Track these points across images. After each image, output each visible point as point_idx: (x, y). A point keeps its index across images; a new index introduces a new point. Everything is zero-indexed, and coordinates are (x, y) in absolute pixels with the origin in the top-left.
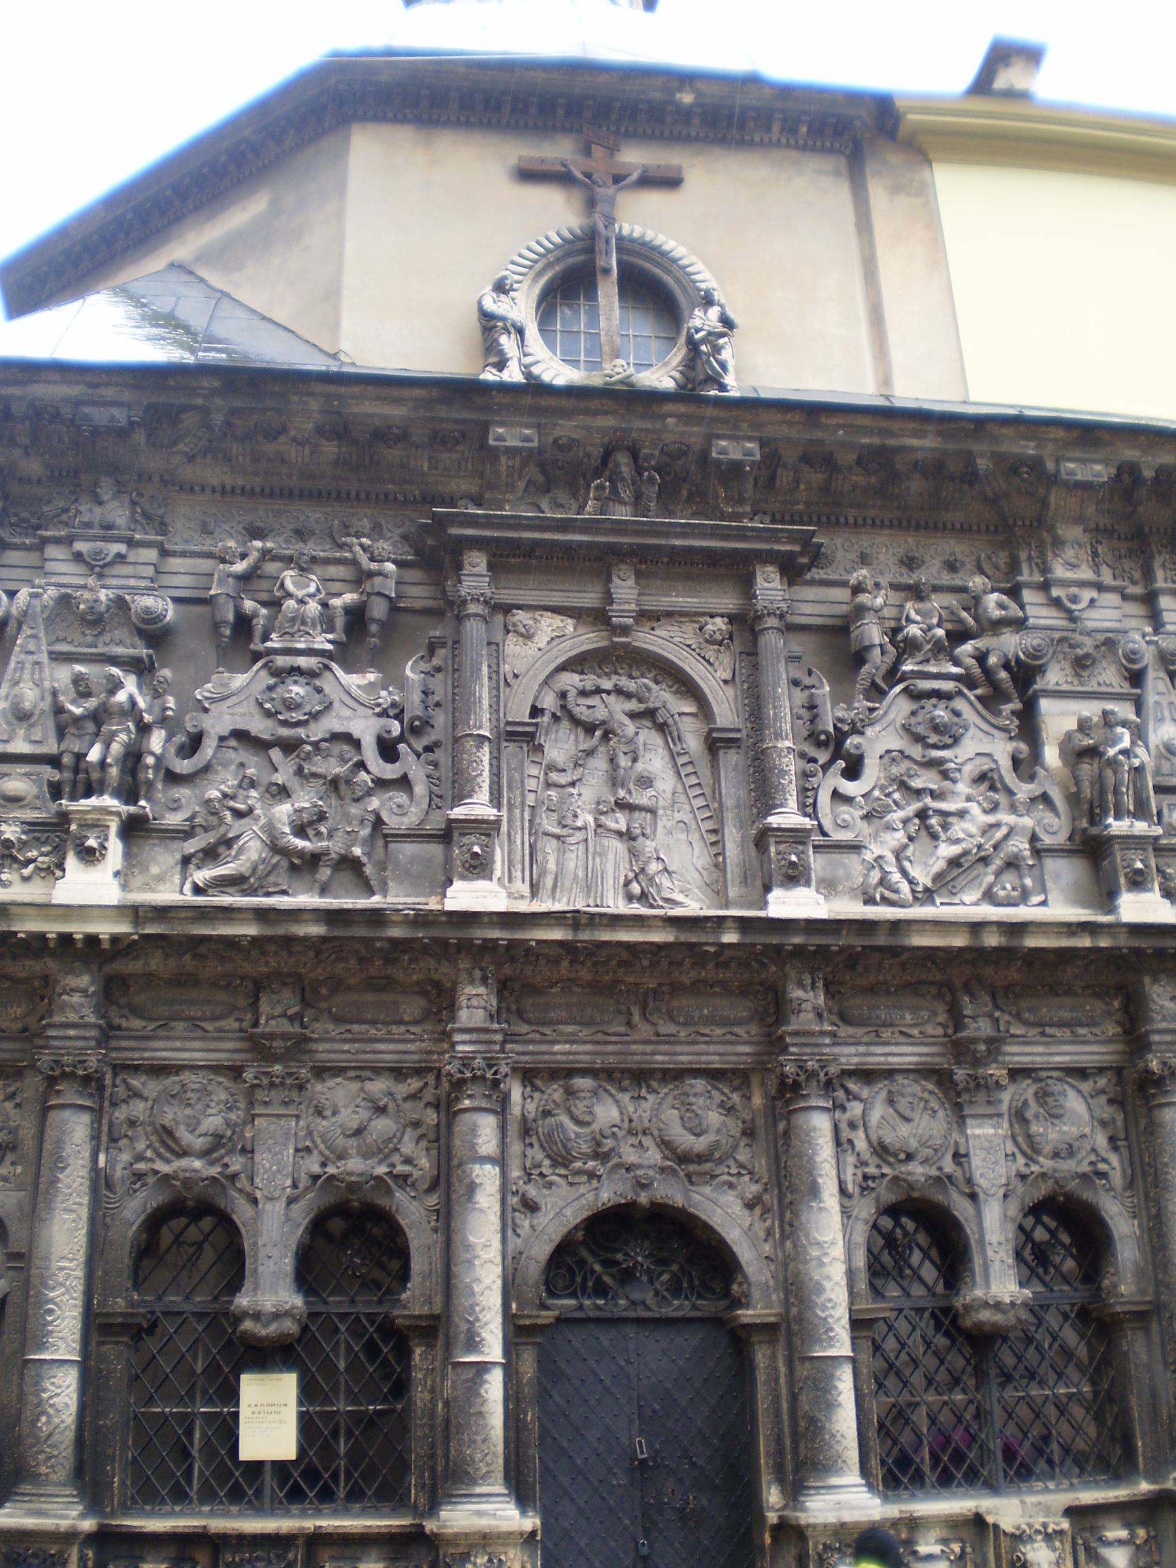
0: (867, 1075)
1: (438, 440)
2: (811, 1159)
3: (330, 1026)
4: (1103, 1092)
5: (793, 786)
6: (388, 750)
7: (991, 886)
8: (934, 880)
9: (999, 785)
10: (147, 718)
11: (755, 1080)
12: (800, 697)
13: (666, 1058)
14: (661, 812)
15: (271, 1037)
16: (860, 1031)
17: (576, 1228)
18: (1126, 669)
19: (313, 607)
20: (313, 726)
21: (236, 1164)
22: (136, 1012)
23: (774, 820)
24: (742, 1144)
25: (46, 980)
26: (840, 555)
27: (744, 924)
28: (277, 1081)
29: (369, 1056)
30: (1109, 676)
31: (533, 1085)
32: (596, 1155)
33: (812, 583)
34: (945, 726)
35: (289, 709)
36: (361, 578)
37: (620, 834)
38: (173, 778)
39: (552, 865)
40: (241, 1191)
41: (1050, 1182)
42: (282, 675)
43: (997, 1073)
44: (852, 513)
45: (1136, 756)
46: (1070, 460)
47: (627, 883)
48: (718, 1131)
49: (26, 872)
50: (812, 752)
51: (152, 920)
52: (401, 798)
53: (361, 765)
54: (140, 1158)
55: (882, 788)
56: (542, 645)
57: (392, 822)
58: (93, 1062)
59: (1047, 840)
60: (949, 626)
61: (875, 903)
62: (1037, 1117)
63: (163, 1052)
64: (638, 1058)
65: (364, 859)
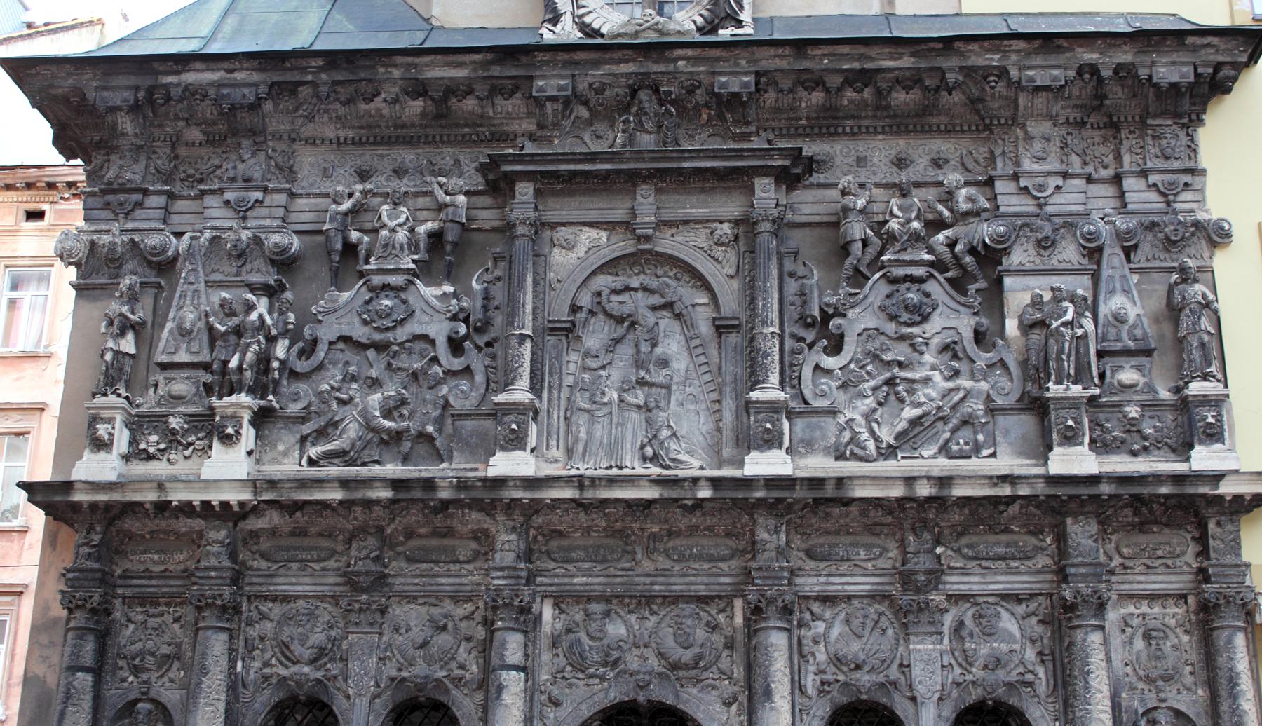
0: (828, 599)
1: (497, 89)
2: (767, 667)
3: (404, 565)
4: (1033, 614)
5: (777, 365)
6: (456, 346)
7: (947, 441)
8: (896, 438)
9: (961, 355)
10: (274, 332)
11: (738, 604)
12: (792, 286)
13: (662, 588)
14: (674, 387)
15: (358, 574)
16: (822, 565)
17: (590, 718)
18: (1084, 248)
19: (402, 235)
20: (399, 331)
21: (335, 669)
22: (264, 556)
23: (754, 395)
24: (724, 655)
25: (200, 534)
26: (839, 160)
27: (715, 482)
28: (364, 607)
29: (434, 588)
30: (1069, 253)
31: (560, 608)
32: (605, 664)
33: (811, 186)
34: (915, 306)
35: (380, 317)
36: (442, 207)
37: (639, 407)
38: (294, 375)
39: (583, 435)
40: (338, 689)
41: (980, 690)
43: (937, 598)
44: (849, 122)
46: (1030, 68)
47: (643, 447)
48: (702, 646)
49: (187, 453)
50: (802, 333)
51: (267, 490)
52: (464, 385)
53: (435, 360)
54: (266, 664)
55: (858, 361)
56: (581, 255)
57: (457, 404)
58: (227, 596)
59: (1000, 401)
60: (930, 217)
61: (847, 459)
62: (971, 635)
63: (283, 586)
64: (639, 588)
65: (435, 435)
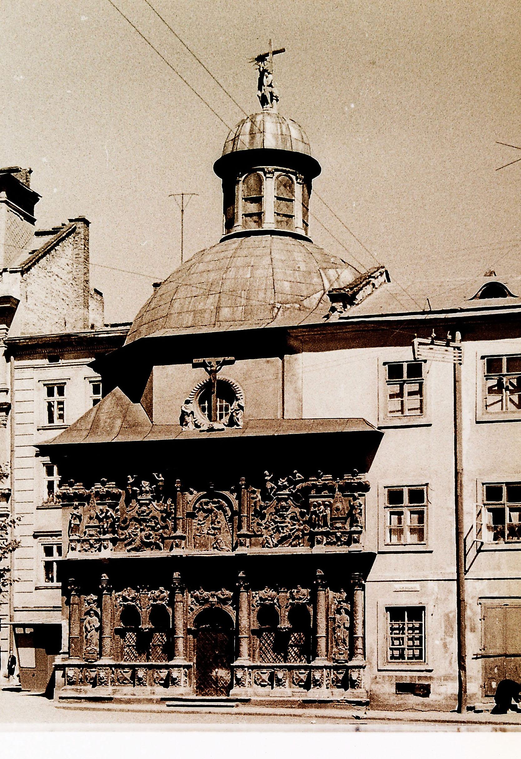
6: (163, 519)
42: (141, 505)
45: (325, 512)
